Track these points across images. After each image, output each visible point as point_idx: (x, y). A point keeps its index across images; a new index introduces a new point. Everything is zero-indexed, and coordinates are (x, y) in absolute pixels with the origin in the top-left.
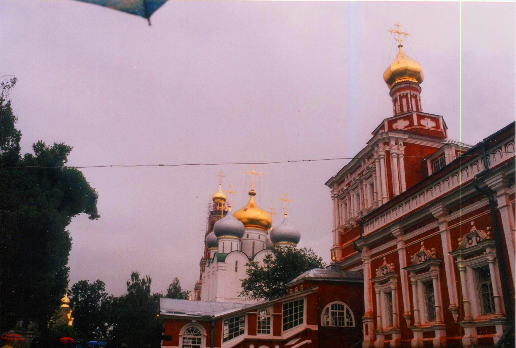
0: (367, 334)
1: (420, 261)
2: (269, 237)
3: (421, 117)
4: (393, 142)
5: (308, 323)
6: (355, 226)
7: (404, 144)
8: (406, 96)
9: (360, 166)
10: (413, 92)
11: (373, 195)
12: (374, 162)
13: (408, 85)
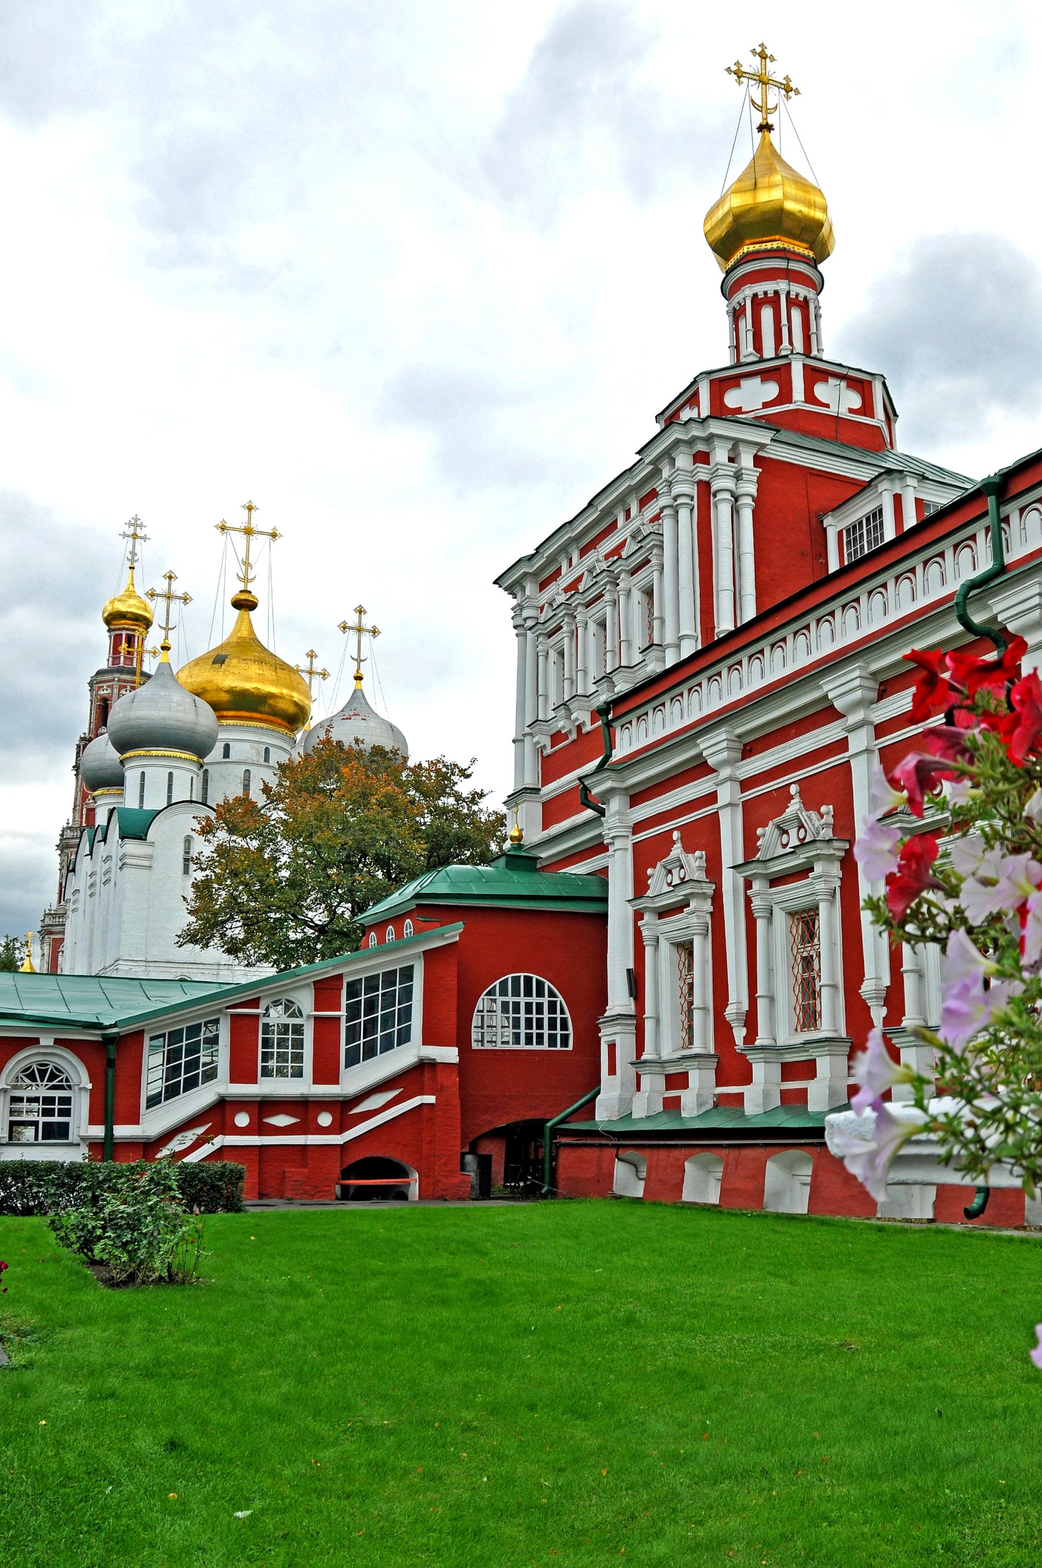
0: (612, 1071)
1: (785, 846)
3: (815, 374)
4: (720, 455)
5: (429, 1039)
6: (588, 728)
7: (758, 460)
8: (774, 301)
10: (800, 290)
11: (651, 627)
12: (657, 518)
13: (781, 264)
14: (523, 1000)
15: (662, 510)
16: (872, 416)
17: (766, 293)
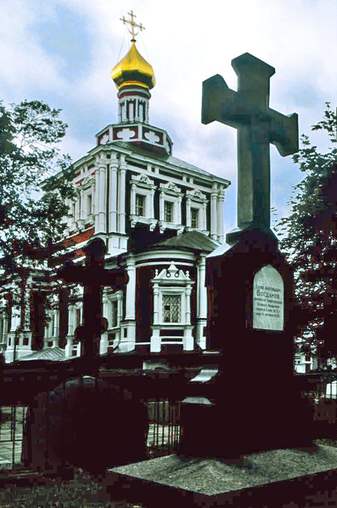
8: (134, 102)
9: (79, 174)
11: (91, 208)
12: (93, 174)
15: (95, 171)
16: (163, 144)
17: (131, 99)
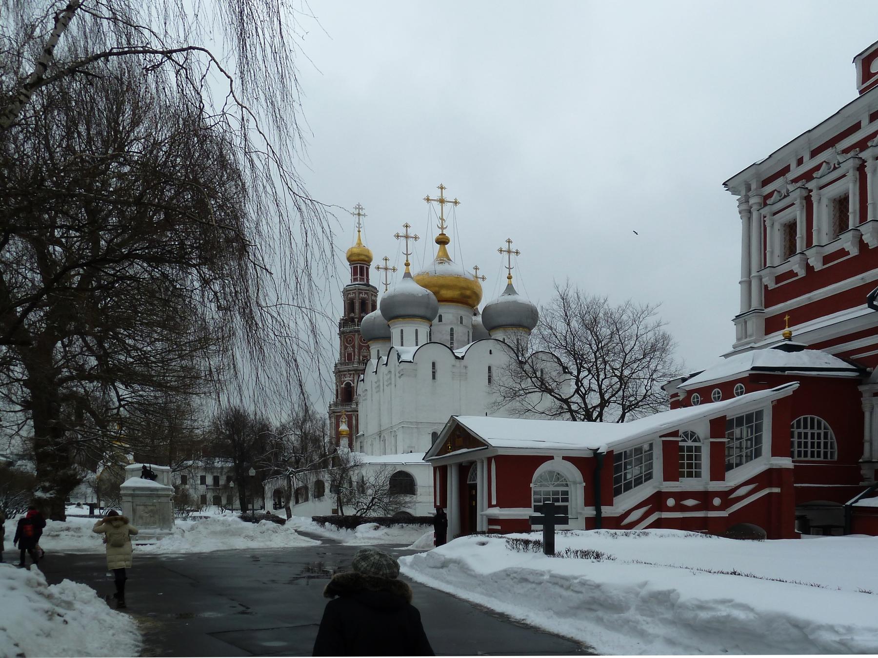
2: (479, 319)
14: (809, 431)
